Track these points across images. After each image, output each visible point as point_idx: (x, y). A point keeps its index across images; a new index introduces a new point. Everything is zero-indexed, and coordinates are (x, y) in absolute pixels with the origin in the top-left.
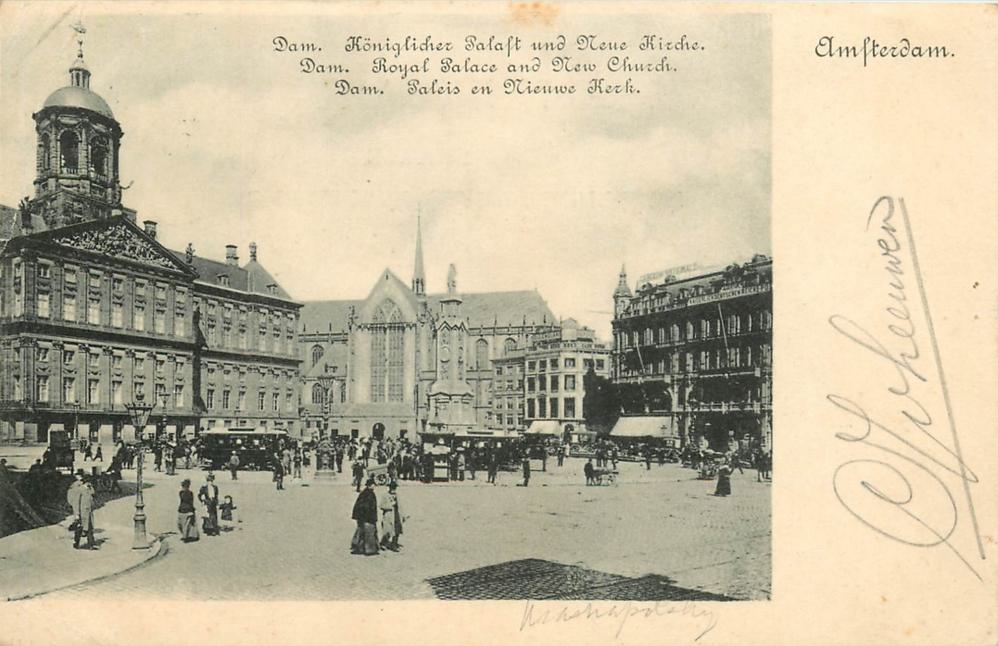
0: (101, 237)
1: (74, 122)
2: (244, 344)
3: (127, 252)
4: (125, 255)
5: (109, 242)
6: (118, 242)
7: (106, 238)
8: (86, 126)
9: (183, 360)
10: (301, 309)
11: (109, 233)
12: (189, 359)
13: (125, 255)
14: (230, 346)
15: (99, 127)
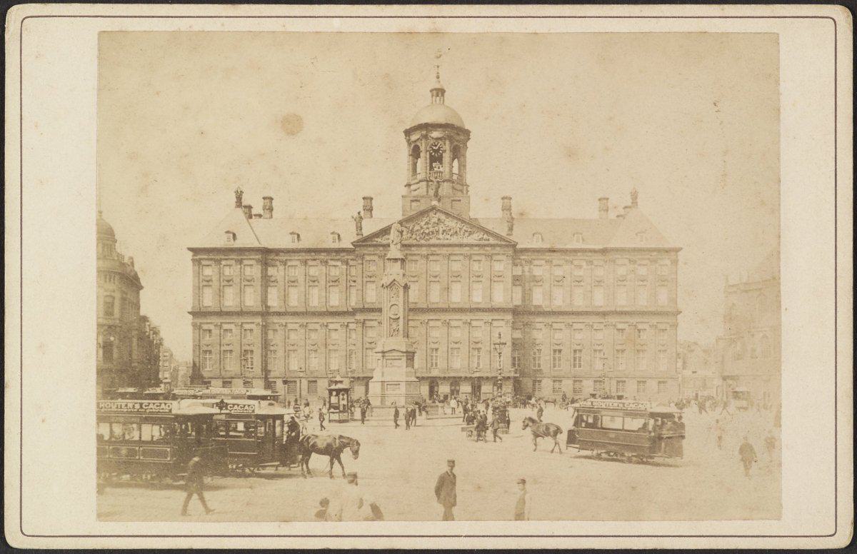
0: (417, 228)
1: (418, 137)
2: (599, 300)
3: (441, 236)
4: (439, 239)
5: (422, 231)
6: (431, 229)
7: (422, 228)
8: (426, 137)
9: (502, 323)
10: (679, 253)
11: (423, 224)
12: (507, 322)
13: (439, 239)
14: (559, 303)
15: (435, 134)
